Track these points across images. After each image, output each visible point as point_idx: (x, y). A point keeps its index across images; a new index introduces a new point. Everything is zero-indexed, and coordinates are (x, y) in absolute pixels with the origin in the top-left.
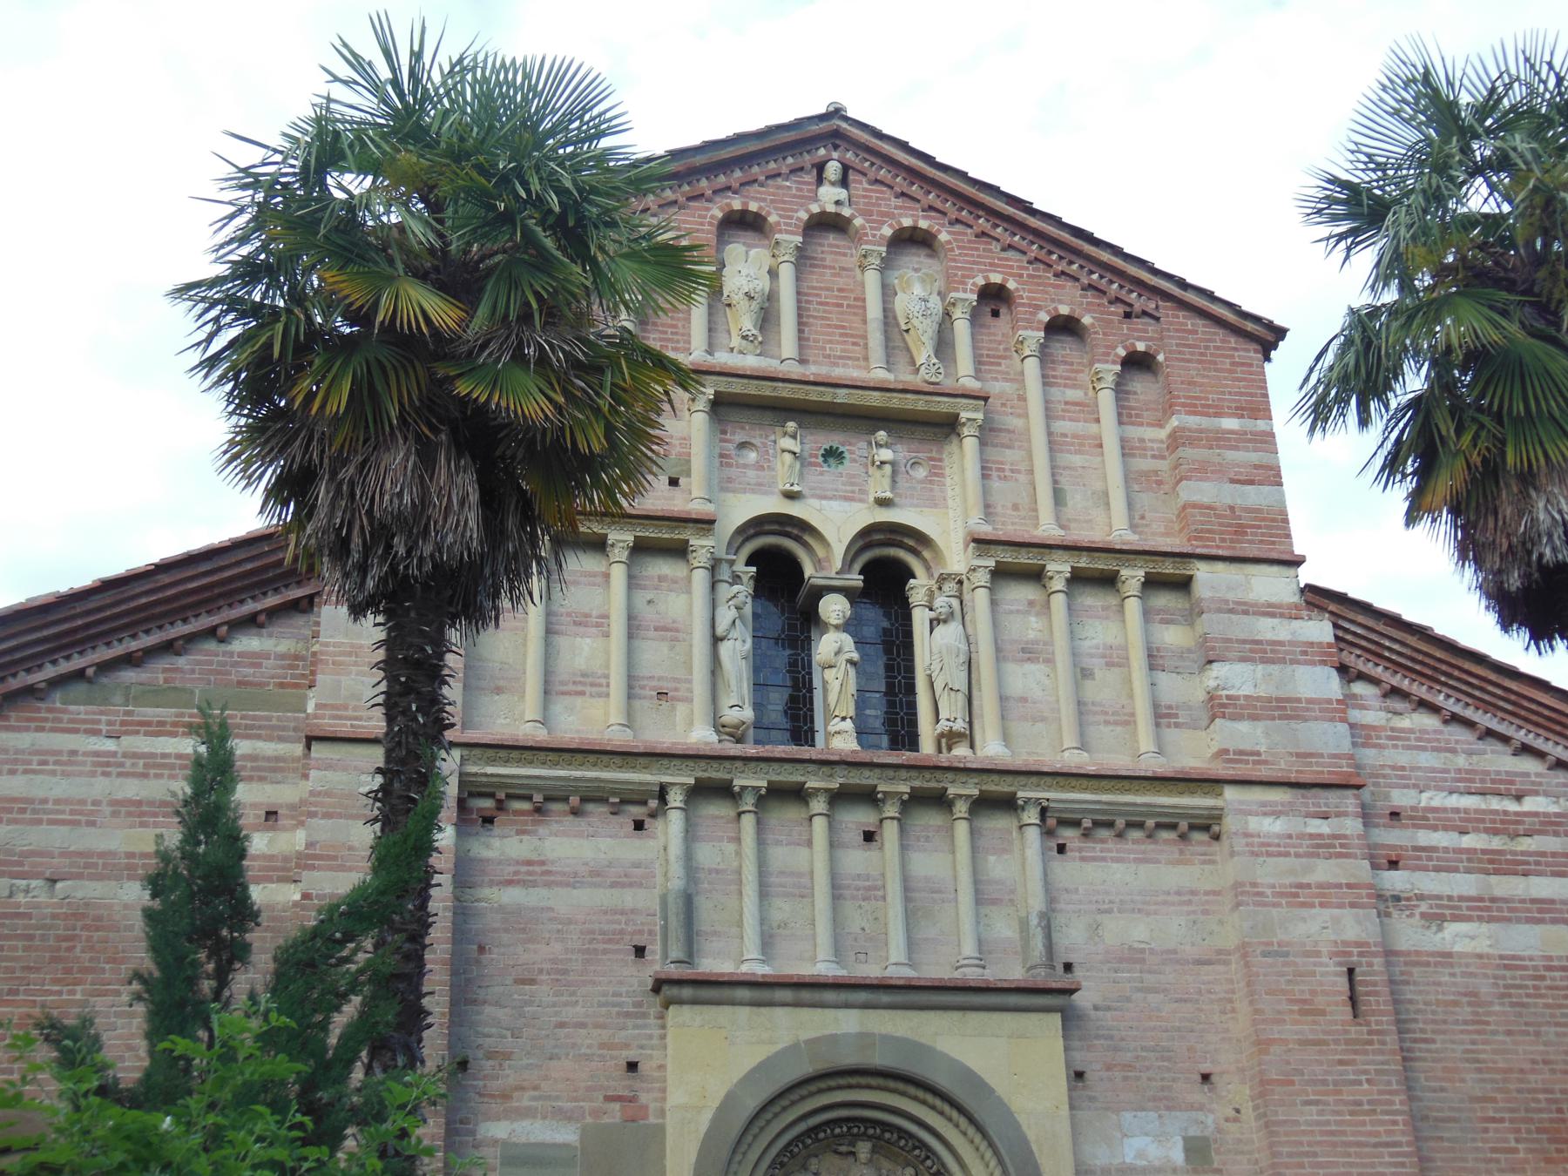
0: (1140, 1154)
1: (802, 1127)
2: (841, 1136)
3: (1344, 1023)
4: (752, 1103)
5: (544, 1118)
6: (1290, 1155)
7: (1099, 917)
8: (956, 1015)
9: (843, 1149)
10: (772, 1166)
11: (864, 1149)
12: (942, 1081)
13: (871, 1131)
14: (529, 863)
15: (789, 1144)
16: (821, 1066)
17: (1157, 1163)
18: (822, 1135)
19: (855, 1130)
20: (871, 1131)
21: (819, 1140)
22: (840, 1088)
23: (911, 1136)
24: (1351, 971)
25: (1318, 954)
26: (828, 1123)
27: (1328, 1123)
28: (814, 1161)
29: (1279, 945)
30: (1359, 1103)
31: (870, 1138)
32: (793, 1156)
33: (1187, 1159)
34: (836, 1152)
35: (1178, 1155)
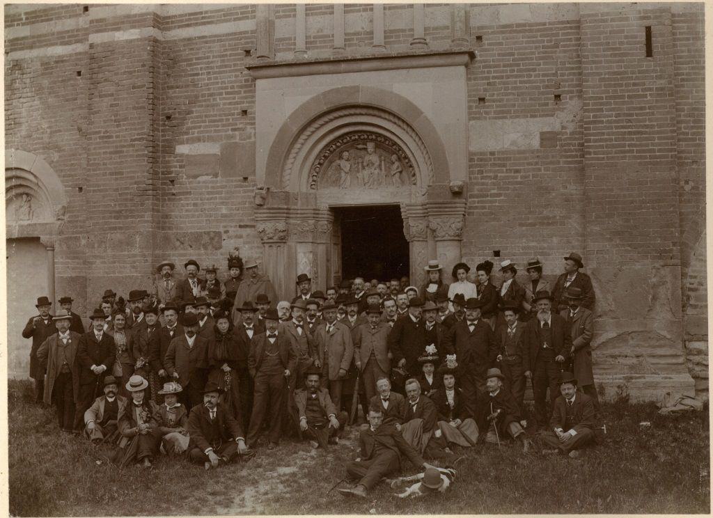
0: (514, 143)
1: (331, 137)
2: (355, 140)
4: (295, 129)
5: (204, 142)
6: (595, 141)
8: (404, 71)
10: (318, 157)
11: (370, 146)
12: (394, 109)
15: (327, 145)
17: (523, 148)
18: (345, 141)
19: (362, 137)
21: (345, 143)
22: (346, 116)
23: (391, 140)
24: (648, 29)
25: (627, 19)
27: (622, 121)
28: (346, 154)
31: (372, 140)
32: (331, 152)
33: (541, 145)
34: (357, 148)
35: (536, 143)
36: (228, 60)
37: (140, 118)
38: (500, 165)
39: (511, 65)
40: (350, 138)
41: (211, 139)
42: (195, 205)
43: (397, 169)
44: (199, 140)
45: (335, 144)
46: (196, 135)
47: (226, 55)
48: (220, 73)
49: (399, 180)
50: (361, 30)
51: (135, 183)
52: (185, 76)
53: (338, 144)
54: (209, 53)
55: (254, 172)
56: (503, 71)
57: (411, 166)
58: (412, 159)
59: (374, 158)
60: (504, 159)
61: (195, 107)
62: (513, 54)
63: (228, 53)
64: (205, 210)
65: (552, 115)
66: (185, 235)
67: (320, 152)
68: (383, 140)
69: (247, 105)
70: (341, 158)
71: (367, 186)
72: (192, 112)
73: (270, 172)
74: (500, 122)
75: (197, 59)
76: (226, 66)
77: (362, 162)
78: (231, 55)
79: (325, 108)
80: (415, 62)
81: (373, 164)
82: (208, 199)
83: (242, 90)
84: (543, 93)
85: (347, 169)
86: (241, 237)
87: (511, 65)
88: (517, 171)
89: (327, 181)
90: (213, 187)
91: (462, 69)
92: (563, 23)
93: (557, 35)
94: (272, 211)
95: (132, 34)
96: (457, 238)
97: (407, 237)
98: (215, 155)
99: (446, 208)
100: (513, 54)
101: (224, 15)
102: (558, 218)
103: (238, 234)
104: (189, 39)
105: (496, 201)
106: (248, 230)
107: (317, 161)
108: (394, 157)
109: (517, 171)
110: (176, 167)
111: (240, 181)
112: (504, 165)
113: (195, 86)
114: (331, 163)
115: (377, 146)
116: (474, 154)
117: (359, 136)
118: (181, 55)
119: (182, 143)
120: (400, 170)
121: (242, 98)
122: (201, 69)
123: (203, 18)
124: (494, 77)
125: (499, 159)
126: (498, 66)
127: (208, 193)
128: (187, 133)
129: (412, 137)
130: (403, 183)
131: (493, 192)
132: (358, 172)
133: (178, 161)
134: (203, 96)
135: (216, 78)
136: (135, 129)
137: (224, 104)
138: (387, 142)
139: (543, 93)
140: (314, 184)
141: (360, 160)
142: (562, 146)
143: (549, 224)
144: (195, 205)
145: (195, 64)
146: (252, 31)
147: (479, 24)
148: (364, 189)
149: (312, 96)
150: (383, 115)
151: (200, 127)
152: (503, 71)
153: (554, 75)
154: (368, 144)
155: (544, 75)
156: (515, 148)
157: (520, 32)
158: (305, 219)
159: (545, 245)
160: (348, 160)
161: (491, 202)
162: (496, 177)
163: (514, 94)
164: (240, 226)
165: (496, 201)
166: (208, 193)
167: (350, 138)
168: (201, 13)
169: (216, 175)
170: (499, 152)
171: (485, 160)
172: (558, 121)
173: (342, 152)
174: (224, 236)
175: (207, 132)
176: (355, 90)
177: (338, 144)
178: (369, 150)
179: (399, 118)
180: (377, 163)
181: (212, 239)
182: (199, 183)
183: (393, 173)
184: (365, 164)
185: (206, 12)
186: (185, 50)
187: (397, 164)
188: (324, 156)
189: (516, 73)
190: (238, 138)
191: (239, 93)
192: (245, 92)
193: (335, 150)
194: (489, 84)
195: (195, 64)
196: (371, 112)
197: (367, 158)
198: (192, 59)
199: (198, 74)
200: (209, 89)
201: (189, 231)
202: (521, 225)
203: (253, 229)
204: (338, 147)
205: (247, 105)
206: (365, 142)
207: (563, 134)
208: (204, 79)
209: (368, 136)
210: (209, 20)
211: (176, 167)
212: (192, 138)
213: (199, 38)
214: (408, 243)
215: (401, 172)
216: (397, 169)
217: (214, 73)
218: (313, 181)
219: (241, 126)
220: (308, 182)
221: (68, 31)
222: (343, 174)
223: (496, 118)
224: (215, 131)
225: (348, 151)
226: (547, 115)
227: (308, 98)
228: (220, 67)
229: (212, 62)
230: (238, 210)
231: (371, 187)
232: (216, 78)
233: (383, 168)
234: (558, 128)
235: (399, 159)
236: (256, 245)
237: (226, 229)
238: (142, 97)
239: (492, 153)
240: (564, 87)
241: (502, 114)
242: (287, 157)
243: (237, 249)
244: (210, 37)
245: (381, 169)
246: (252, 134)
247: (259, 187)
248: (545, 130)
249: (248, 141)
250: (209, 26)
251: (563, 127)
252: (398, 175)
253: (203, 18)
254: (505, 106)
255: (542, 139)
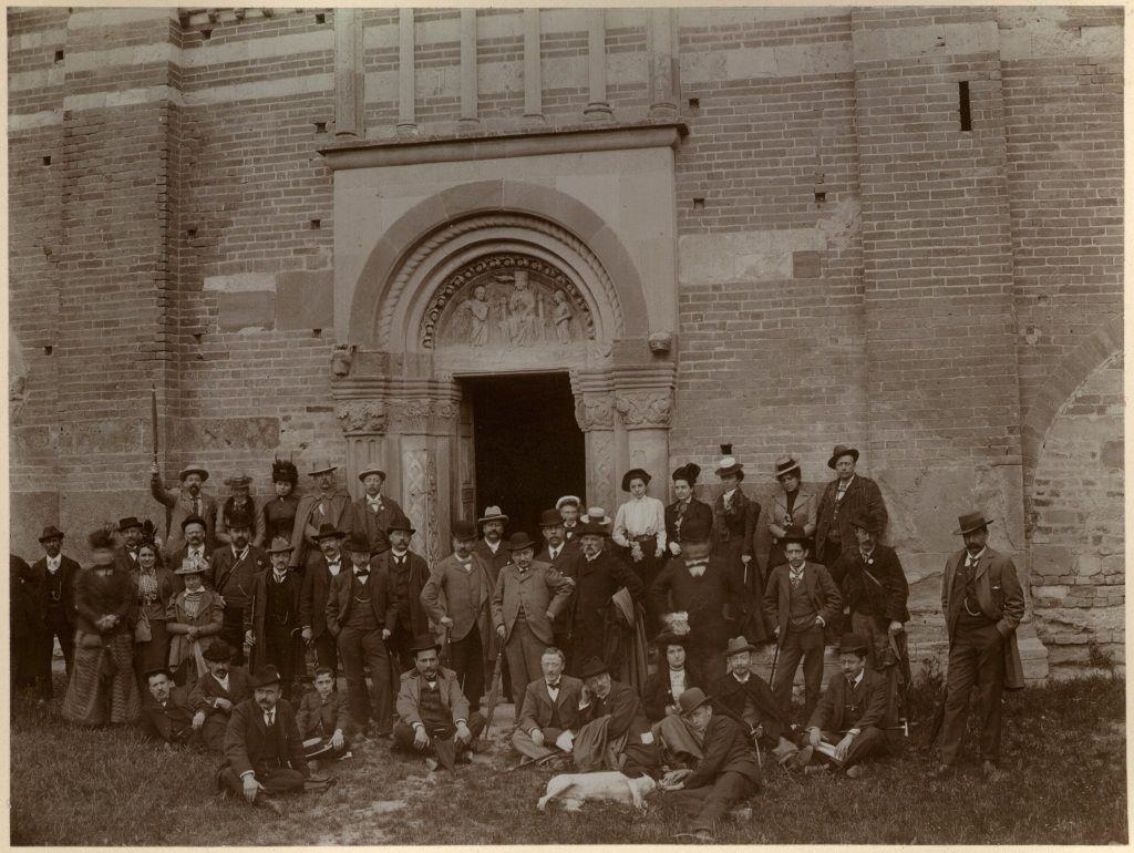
0: (752, 271)
1: (458, 262)
2: (496, 267)
3: (951, 136)
4: (398, 250)
5: (250, 271)
6: (883, 266)
7: (730, 54)
8: (573, 157)
9: (504, 278)
11: (520, 277)
13: (520, 263)
14: (237, 64)
15: (449, 277)
16: (456, 212)
17: (766, 278)
18: (479, 269)
19: (507, 263)
20: (520, 263)
24: (964, 86)
26: (482, 257)
27: (923, 233)
28: (480, 290)
29: (889, 64)
30: (959, 212)
31: (523, 268)
32: (457, 288)
33: (795, 274)
34: (498, 281)
35: (787, 270)
36: (290, 140)
37: (145, 233)
38: (728, 307)
39: (744, 146)
40: (488, 264)
41: (259, 267)
42: (235, 374)
43: (563, 314)
44: (241, 268)
45: (463, 275)
46: (237, 260)
47: (286, 131)
48: (278, 159)
49: (566, 332)
50: (504, 90)
51: (138, 339)
52: (220, 165)
53: (469, 274)
54: (258, 126)
55: (331, 322)
56: (732, 156)
57: (586, 310)
58: (587, 298)
59: (527, 297)
60: (740, 296)
61: (235, 214)
62: (748, 128)
63: (289, 127)
64: (252, 382)
65: (812, 226)
66: (219, 424)
67: (439, 287)
68: (540, 266)
69: (321, 211)
70: (472, 296)
71: (515, 342)
72: (231, 223)
73: (356, 321)
74: (728, 236)
75: (238, 137)
76: (286, 149)
77: (507, 304)
78: (293, 131)
79: (447, 216)
80: (592, 141)
81: (525, 307)
82: (256, 365)
83: (312, 188)
84: (798, 191)
85: (482, 315)
86: (310, 426)
87: (744, 146)
88: (757, 316)
89: (451, 334)
90: (264, 345)
91: (668, 152)
92: (827, 76)
93: (819, 96)
94: (361, 384)
95: (134, 97)
96: (661, 425)
97: (581, 425)
98: (268, 293)
99: (644, 376)
100: (748, 128)
101: (283, 67)
102: (824, 390)
103: (305, 421)
104: (227, 105)
105: (723, 365)
106: (323, 416)
107: (435, 303)
108: (559, 295)
109: (757, 316)
110: (203, 312)
111: (308, 335)
112: (737, 307)
113: (235, 181)
114: (457, 304)
115: (532, 277)
116: (687, 289)
117: (502, 262)
118: (214, 131)
119: (212, 274)
120: (568, 315)
121: (313, 200)
122: (246, 153)
123: (250, 71)
124: (718, 166)
125: (728, 297)
126: (726, 147)
127: (257, 355)
128: (223, 258)
129: (587, 262)
130: (573, 336)
131: (718, 349)
132: (500, 319)
133: (207, 303)
134: (249, 197)
135: (270, 168)
136: (137, 251)
137: (283, 210)
138: (547, 271)
139: (798, 191)
140: (429, 339)
141: (504, 300)
142: (828, 274)
143: (810, 401)
144: (235, 374)
145: (235, 145)
146: (327, 92)
147: (694, 80)
148: (508, 347)
149: (425, 198)
150: (540, 226)
151: (243, 248)
152: (732, 156)
153: (817, 160)
154: (516, 273)
155: (798, 162)
156: (754, 279)
157: (757, 92)
158: (414, 396)
159: (804, 435)
160: (484, 300)
161: (716, 366)
162: (723, 326)
163: (750, 193)
164: (309, 410)
165: (723, 365)
166: (257, 355)
167: (488, 264)
168: (246, 63)
169: (269, 326)
170: (727, 286)
171: (704, 298)
172: (823, 233)
173: (474, 287)
174: (283, 426)
175: (254, 255)
176: (494, 187)
177: (469, 274)
178: (517, 284)
179: (567, 232)
180: (532, 305)
181: (263, 430)
182: (242, 337)
183: (556, 320)
184: (511, 306)
185: (254, 62)
186: (219, 123)
187: (563, 305)
188: (445, 294)
189: (753, 158)
190: (305, 265)
191: (307, 192)
192: (316, 191)
193: (462, 284)
194: (710, 176)
195: (235, 145)
196: (521, 222)
197: (515, 297)
198: (230, 137)
199: (240, 162)
200: (257, 187)
201: (226, 418)
202: (766, 403)
203: (330, 413)
204: (467, 279)
205: (321, 211)
206: (511, 270)
207: (828, 255)
208: (250, 171)
209: (516, 261)
210: (259, 74)
211: (203, 312)
212: (231, 265)
213: (242, 102)
214: (583, 435)
215: (569, 319)
216: (563, 314)
217: (267, 160)
218: (428, 334)
219: (310, 245)
220: (419, 336)
221: (30, 92)
222: (476, 323)
223: (722, 231)
224: (268, 254)
225: (483, 286)
226: (804, 225)
227: (417, 200)
228: (278, 150)
229: (263, 142)
230: (306, 383)
231: (522, 343)
232: (270, 168)
233: (541, 312)
234: (821, 245)
235: (567, 298)
236: (334, 439)
237: (286, 414)
238: (148, 199)
239: (716, 288)
240: (832, 179)
241: (733, 223)
242: (384, 295)
243: (304, 446)
244: (260, 101)
245: (537, 315)
246: (328, 260)
247: (340, 345)
248: (801, 248)
249: (322, 269)
250: (258, 83)
251: (830, 244)
252: (564, 324)
253: (250, 71)
254: (737, 211)
255: (796, 264)
